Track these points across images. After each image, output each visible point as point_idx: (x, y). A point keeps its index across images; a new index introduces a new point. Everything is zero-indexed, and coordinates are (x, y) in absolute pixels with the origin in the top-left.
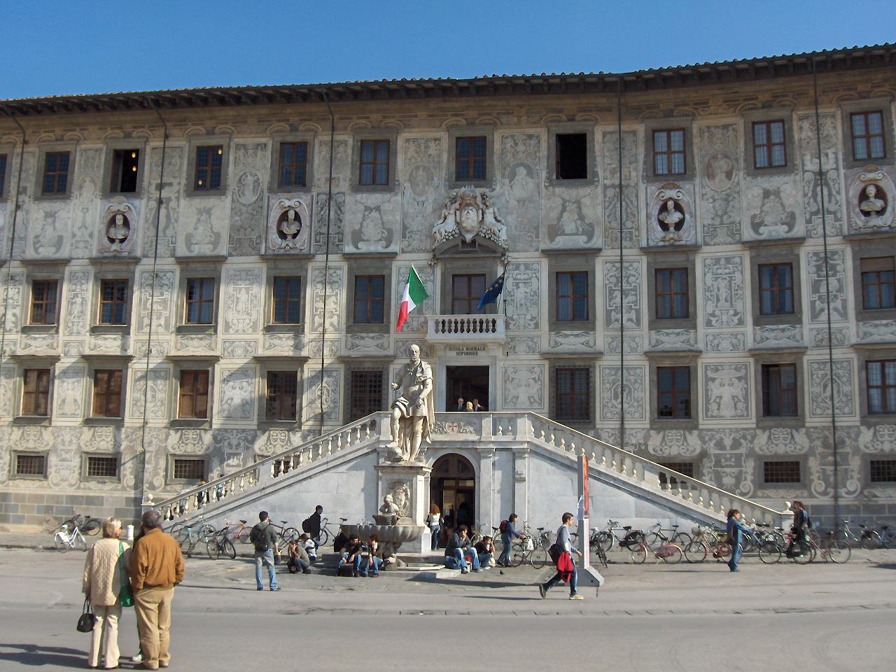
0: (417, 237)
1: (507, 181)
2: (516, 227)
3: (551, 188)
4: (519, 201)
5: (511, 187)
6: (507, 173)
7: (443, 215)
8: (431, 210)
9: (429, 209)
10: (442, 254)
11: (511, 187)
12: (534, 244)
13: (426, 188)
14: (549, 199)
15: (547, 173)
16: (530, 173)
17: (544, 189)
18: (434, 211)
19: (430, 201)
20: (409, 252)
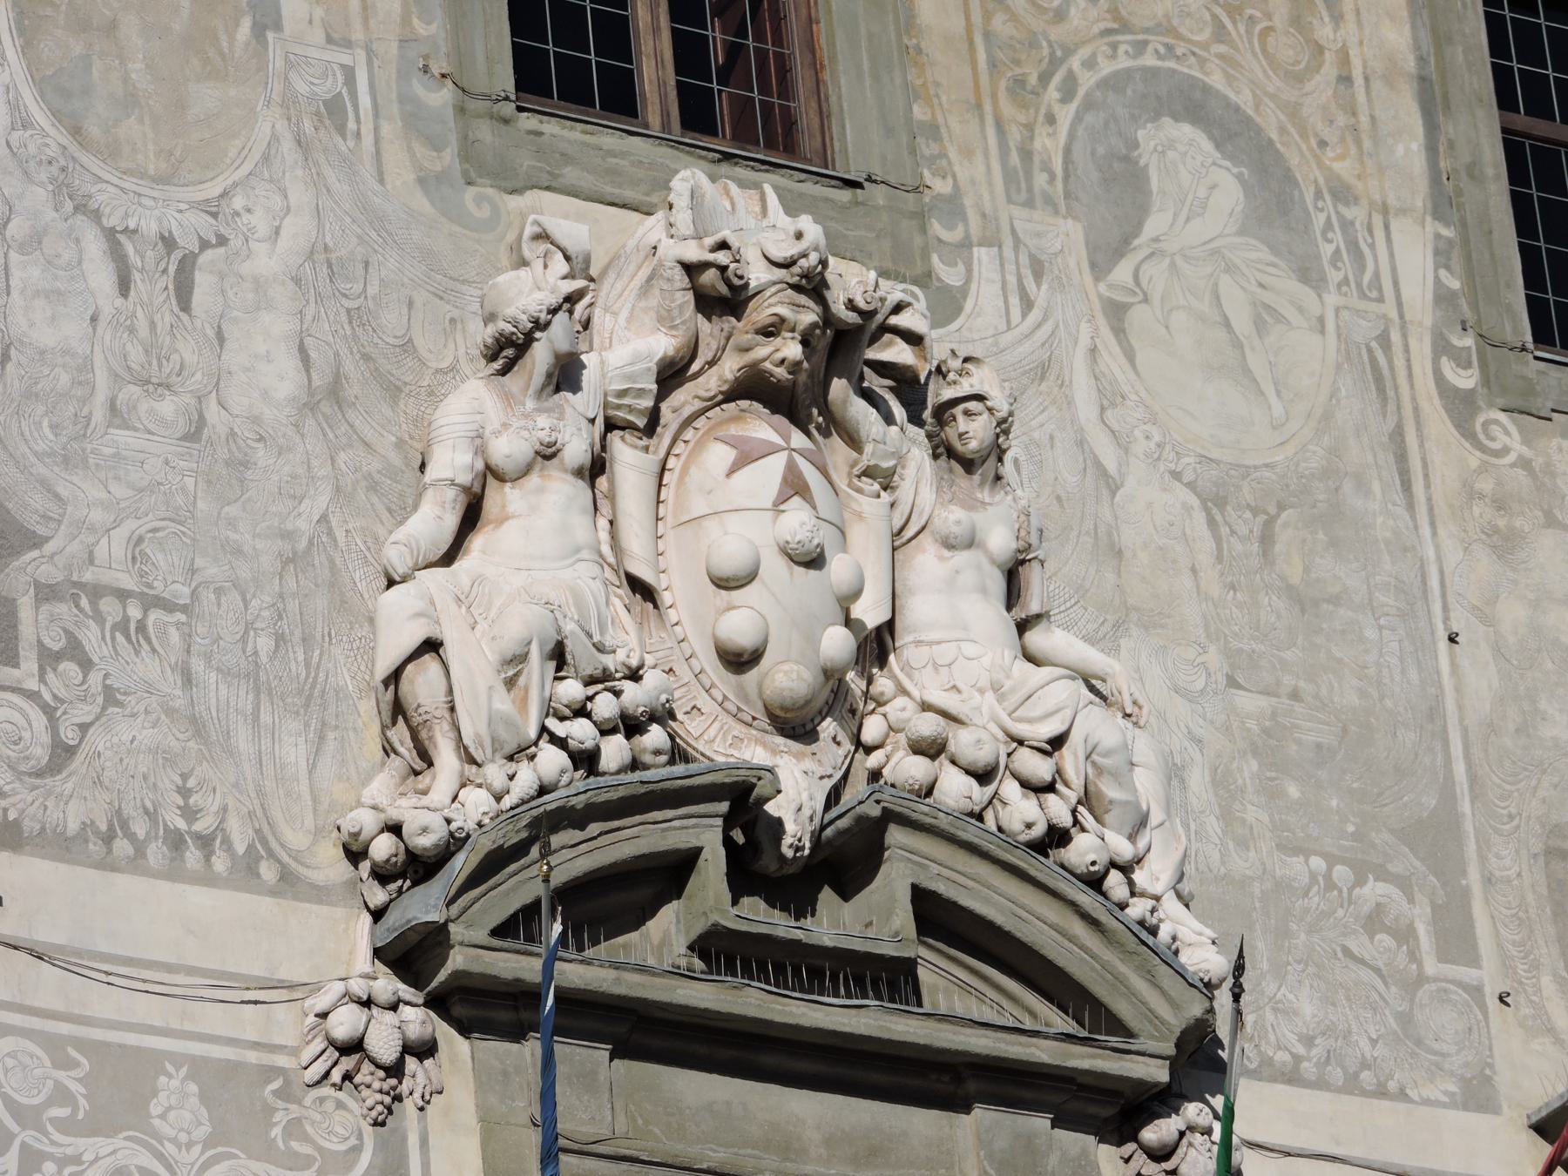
0: (147, 667)
1: (1065, 238)
2: (1221, 780)
3: (1506, 431)
4: (1214, 502)
5: (1116, 312)
6: (1049, 144)
7: (452, 463)
8: (282, 379)
9: (264, 371)
10: (518, 927)
11: (1116, 312)
12: (1442, 1022)
13: (205, 96)
14: (1505, 544)
15: (1442, 255)
16: (1274, 198)
17: (1438, 421)
18: (326, 397)
19: (265, 262)
20: (60, 845)
